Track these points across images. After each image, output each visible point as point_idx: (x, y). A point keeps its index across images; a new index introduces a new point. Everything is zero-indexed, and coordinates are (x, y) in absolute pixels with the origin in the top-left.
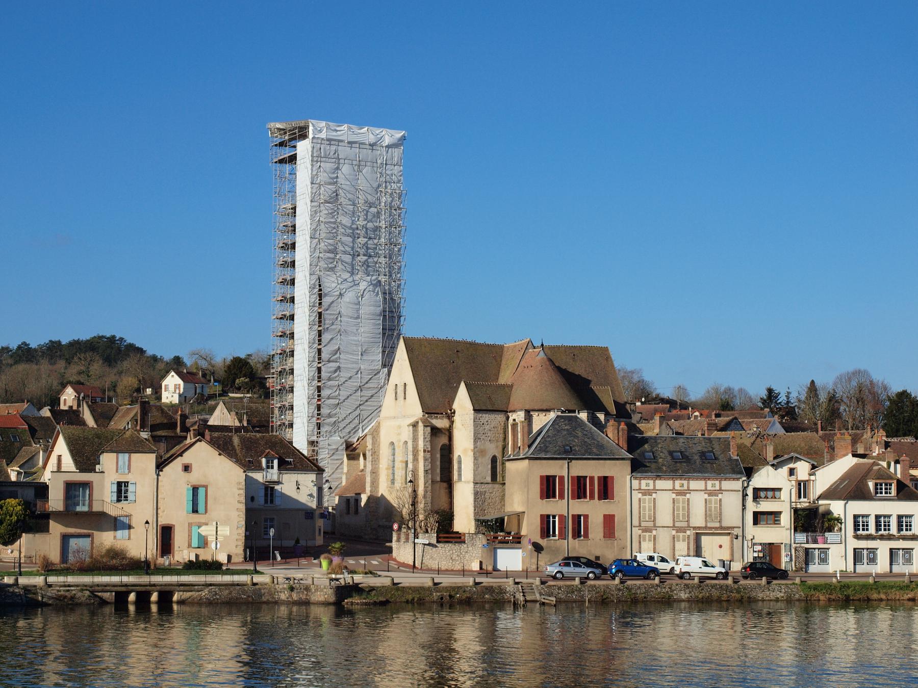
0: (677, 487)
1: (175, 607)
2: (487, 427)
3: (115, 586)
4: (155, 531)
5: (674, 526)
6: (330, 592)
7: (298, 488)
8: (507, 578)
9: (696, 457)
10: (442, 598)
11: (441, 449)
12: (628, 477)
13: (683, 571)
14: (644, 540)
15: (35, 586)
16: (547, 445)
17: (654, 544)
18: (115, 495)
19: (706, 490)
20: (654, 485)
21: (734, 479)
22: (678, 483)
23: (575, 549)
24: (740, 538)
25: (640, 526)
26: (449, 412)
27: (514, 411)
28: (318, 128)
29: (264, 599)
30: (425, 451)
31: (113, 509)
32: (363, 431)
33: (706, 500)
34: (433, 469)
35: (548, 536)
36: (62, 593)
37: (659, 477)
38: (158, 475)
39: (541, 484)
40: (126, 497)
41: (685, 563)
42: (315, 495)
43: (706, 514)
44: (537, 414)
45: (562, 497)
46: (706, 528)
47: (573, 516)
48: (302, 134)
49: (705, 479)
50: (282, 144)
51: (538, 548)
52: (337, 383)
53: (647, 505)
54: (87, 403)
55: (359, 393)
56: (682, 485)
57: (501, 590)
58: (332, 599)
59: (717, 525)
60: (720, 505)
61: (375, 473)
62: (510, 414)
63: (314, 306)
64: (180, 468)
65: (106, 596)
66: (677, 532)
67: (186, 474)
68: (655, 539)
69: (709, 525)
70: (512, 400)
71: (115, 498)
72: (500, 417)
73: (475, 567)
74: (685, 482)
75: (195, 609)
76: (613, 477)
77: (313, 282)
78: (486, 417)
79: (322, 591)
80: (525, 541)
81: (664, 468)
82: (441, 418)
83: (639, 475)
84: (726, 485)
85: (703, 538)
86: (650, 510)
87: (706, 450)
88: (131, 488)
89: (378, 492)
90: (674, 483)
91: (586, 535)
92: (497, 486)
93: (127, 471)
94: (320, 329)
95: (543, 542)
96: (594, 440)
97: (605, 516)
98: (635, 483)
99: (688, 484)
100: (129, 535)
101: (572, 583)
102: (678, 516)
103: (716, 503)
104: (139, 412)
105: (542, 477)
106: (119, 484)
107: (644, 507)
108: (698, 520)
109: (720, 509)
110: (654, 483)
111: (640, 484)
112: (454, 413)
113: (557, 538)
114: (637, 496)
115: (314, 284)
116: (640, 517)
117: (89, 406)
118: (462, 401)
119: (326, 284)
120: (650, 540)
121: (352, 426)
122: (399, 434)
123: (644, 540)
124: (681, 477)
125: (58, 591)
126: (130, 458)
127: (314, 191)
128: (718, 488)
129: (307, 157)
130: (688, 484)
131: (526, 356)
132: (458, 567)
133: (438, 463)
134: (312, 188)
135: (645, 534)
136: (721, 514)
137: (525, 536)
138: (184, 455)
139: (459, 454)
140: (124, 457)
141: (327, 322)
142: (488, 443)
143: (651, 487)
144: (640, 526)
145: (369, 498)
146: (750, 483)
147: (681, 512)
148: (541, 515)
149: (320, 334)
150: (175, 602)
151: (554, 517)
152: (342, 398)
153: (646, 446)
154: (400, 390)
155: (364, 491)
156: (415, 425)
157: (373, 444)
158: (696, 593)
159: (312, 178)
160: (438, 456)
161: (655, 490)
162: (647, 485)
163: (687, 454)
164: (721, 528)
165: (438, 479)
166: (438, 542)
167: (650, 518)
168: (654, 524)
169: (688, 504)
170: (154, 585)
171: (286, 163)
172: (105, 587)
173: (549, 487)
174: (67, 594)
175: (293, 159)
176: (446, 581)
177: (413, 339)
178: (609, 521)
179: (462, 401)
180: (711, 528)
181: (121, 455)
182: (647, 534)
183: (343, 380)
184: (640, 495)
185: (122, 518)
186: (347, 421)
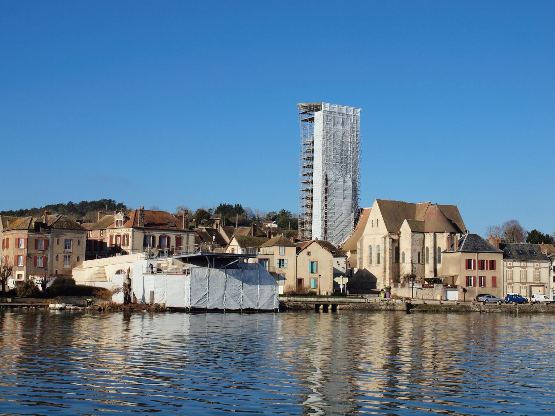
0: (522, 265)
1: (338, 311)
2: (417, 239)
3: (314, 302)
4: (295, 281)
5: (521, 282)
6: (405, 306)
7: (339, 264)
8: (465, 302)
9: (528, 253)
10: (446, 310)
11: (395, 249)
12: (502, 261)
13: (537, 300)
14: (509, 288)
15: (284, 301)
16: (467, 246)
17: (513, 290)
18: (279, 265)
19: (534, 267)
20: (513, 264)
21: (545, 262)
22: (522, 263)
23: (480, 291)
24: (548, 288)
25: (507, 282)
26: (398, 232)
27: (428, 233)
28: (326, 107)
29: (375, 308)
30: (389, 249)
31: (278, 271)
32: (344, 241)
33: (534, 271)
34: (392, 257)
35: (469, 285)
36: (295, 304)
37: (515, 261)
38: (297, 256)
39: (466, 263)
40: (283, 266)
41: (537, 297)
42: (345, 267)
43: (534, 277)
44: (438, 234)
45: (474, 268)
46: (534, 283)
47: (479, 277)
48: (318, 109)
49: (534, 262)
50: (305, 113)
51: (465, 291)
52: (333, 219)
53: (510, 273)
54: (221, 226)
55: (342, 224)
56: (524, 265)
57: (469, 307)
58: (405, 309)
59: (538, 282)
60: (540, 273)
61: (361, 259)
62: (426, 234)
63: (323, 185)
64: (306, 253)
65: (312, 306)
66: (522, 284)
67: (309, 256)
68: (513, 287)
69: (535, 282)
70: (425, 228)
71: (279, 266)
72: (421, 235)
73: (439, 298)
74: (525, 263)
75: (346, 312)
76: (495, 261)
77: (323, 174)
78: (416, 235)
79: (401, 305)
80: (459, 288)
81: (516, 257)
82: (395, 235)
83: (506, 260)
84: (543, 265)
85: (532, 287)
86: (511, 275)
87: (531, 250)
88: (285, 262)
89: (362, 267)
90: (521, 264)
91: (484, 285)
92: (420, 265)
93: (284, 254)
94: (326, 195)
95: (467, 288)
96: (486, 244)
97: (492, 277)
98: (505, 263)
99: (527, 264)
100: (285, 282)
101: (496, 304)
102: (523, 278)
103: (538, 273)
104: (252, 230)
105: (466, 260)
106: (280, 260)
107: (509, 273)
108: (531, 279)
109: (540, 275)
110: (513, 263)
111: (507, 264)
112: (401, 233)
113: (472, 286)
114: (505, 269)
115: (324, 175)
116: (507, 278)
117: (222, 227)
118: (405, 228)
119: (330, 176)
120: (511, 288)
121: (339, 238)
122: (374, 242)
123: (509, 288)
124: (524, 261)
125: (293, 303)
126: (285, 248)
127: (324, 134)
128: (539, 266)
129: (321, 119)
130: (527, 264)
131: (429, 209)
132: (432, 298)
133: (394, 255)
134: (323, 133)
136: (540, 277)
137: (459, 285)
138: (307, 248)
139: (403, 251)
140: (282, 248)
141: (330, 192)
142: (417, 246)
143: (512, 265)
144: (507, 282)
145: (359, 271)
146: (553, 264)
147: (524, 276)
148: (466, 276)
149: (326, 197)
150: (338, 309)
151: (471, 277)
152: (335, 226)
153: (506, 248)
154: (375, 222)
155: (356, 267)
156: (385, 238)
157: (361, 246)
158: (546, 310)
159: (324, 128)
160: (394, 251)
161: (513, 266)
162: (510, 264)
163: (523, 251)
164: (540, 283)
165: (394, 261)
166: (423, 287)
167: (511, 278)
168: (513, 281)
169: (527, 273)
170: (330, 302)
171: (308, 121)
172: (311, 302)
173: (469, 264)
174: (297, 304)
175: (312, 120)
176: (429, 302)
177: (380, 200)
178: (494, 279)
179: (405, 228)
180: (536, 283)
181: (281, 247)
182: (510, 285)
183: (336, 218)
184: (507, 269)
185: (281, 275)
186: (337, 236)
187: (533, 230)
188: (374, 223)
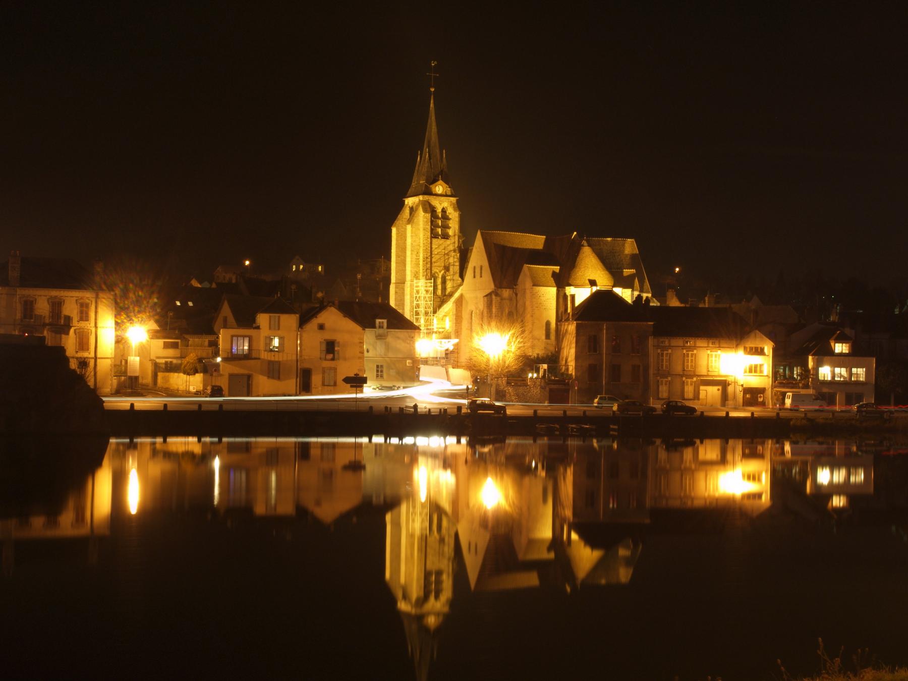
17: (669, 387)
64: (316, 328)
86: (666, 362)
110: (669, 341)
120: (666, 384)
123: (662, 384)
135: (662, 379)
147: (690, 364)
161: (670, 347)
188: (476, 271)
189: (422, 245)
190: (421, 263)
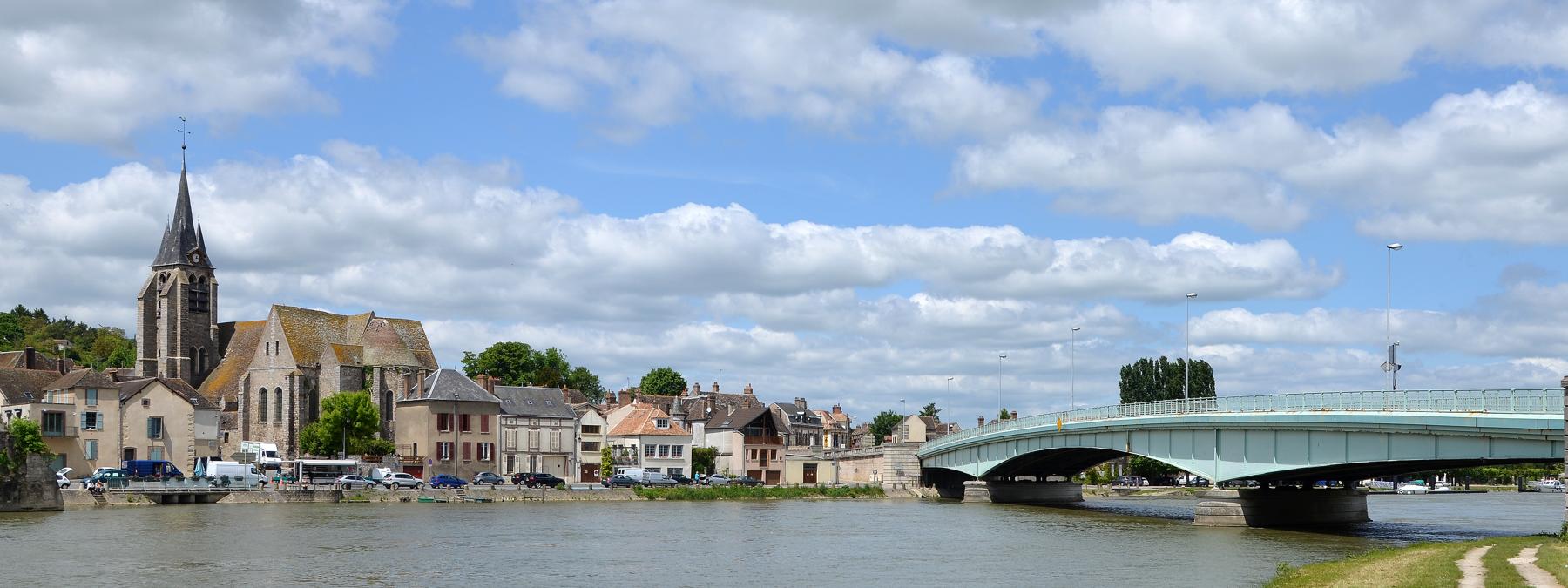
45: (452, 428)
64: (140, 402)
88: (98, 418)
107: (509, 438)
108: (545, 448)
151: (446, 444)
154: (272, 347)
187: (1132, 361)
189: (179, 318)
190: (179, 337)
